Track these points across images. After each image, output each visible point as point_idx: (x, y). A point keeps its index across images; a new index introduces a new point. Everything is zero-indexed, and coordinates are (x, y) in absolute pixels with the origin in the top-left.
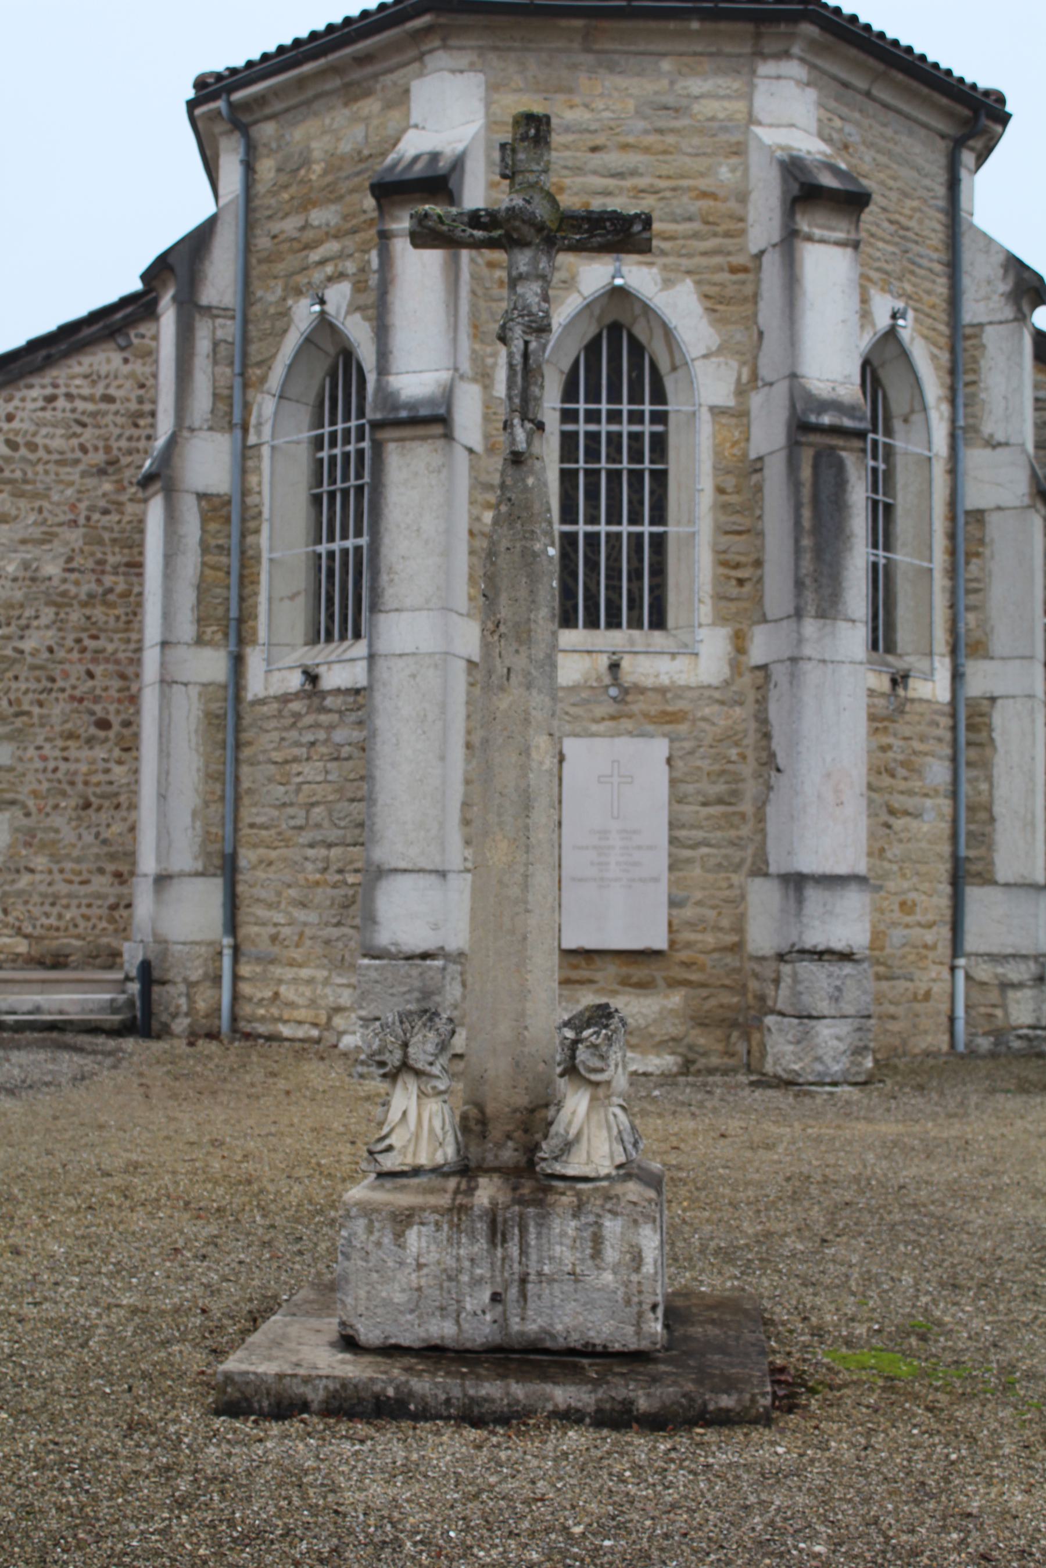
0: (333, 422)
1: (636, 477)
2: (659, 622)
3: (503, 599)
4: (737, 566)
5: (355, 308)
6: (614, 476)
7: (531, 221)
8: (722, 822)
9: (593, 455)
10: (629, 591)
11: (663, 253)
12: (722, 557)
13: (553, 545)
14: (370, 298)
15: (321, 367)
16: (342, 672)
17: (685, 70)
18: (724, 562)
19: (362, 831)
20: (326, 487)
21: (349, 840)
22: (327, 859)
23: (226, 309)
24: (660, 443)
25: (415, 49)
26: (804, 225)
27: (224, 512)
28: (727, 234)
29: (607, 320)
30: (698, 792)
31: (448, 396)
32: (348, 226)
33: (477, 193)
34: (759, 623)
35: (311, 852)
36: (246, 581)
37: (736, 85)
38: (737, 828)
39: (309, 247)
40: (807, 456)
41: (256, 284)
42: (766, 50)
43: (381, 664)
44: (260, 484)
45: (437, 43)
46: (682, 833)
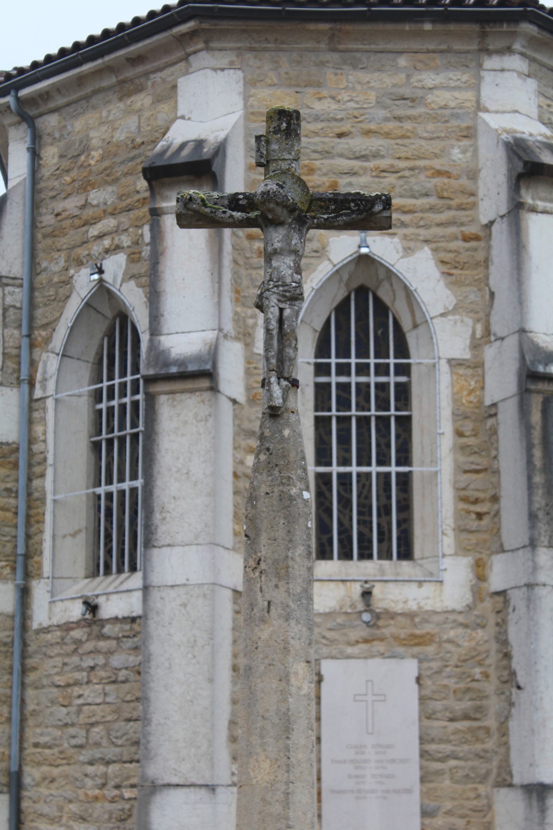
0: (111, 377)
1: (383, 422)
2: (406, 553)
3: (264, 539)
4: (476, 501)
5: (129, 276)
6: (363, 422)
7: (285, 204)
8: (469, 736)
9: (343, 404)
10: (379, 525)
11: (404, 225)
12: (462, 493)
13: (307, 489)
14: (143, 267)
15: (99, 328)
16: (119, 600)
17: (419, 65)
18: (463, 498)
19: (137, 749)
20: (104, 435)
21: (125, 758)
22: (105, 776)
23: (14, 278)
24: (404, 393)
25: (182, 51)
26: (528, 198)
27: (12, 459)
28: (460, 208)
29: (355, 285)
30: (446, 709)
31: (213, 353)
32: (124, 204)
33: (237, 177)
34: (497, 552)
35: (90, 769)
36: (32, 520)
37: (465, 78)
38: (483, 742)
39: (87, 223)
40: (536, 402)
41: (41, 255)
42: (491, 47)
43: (155, 594)
44: (45, 433)
45: (201, 45)
46: (432, 747)
